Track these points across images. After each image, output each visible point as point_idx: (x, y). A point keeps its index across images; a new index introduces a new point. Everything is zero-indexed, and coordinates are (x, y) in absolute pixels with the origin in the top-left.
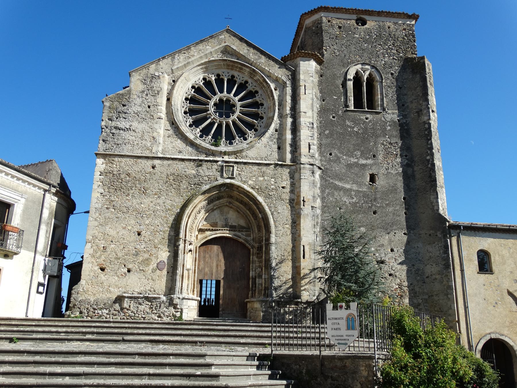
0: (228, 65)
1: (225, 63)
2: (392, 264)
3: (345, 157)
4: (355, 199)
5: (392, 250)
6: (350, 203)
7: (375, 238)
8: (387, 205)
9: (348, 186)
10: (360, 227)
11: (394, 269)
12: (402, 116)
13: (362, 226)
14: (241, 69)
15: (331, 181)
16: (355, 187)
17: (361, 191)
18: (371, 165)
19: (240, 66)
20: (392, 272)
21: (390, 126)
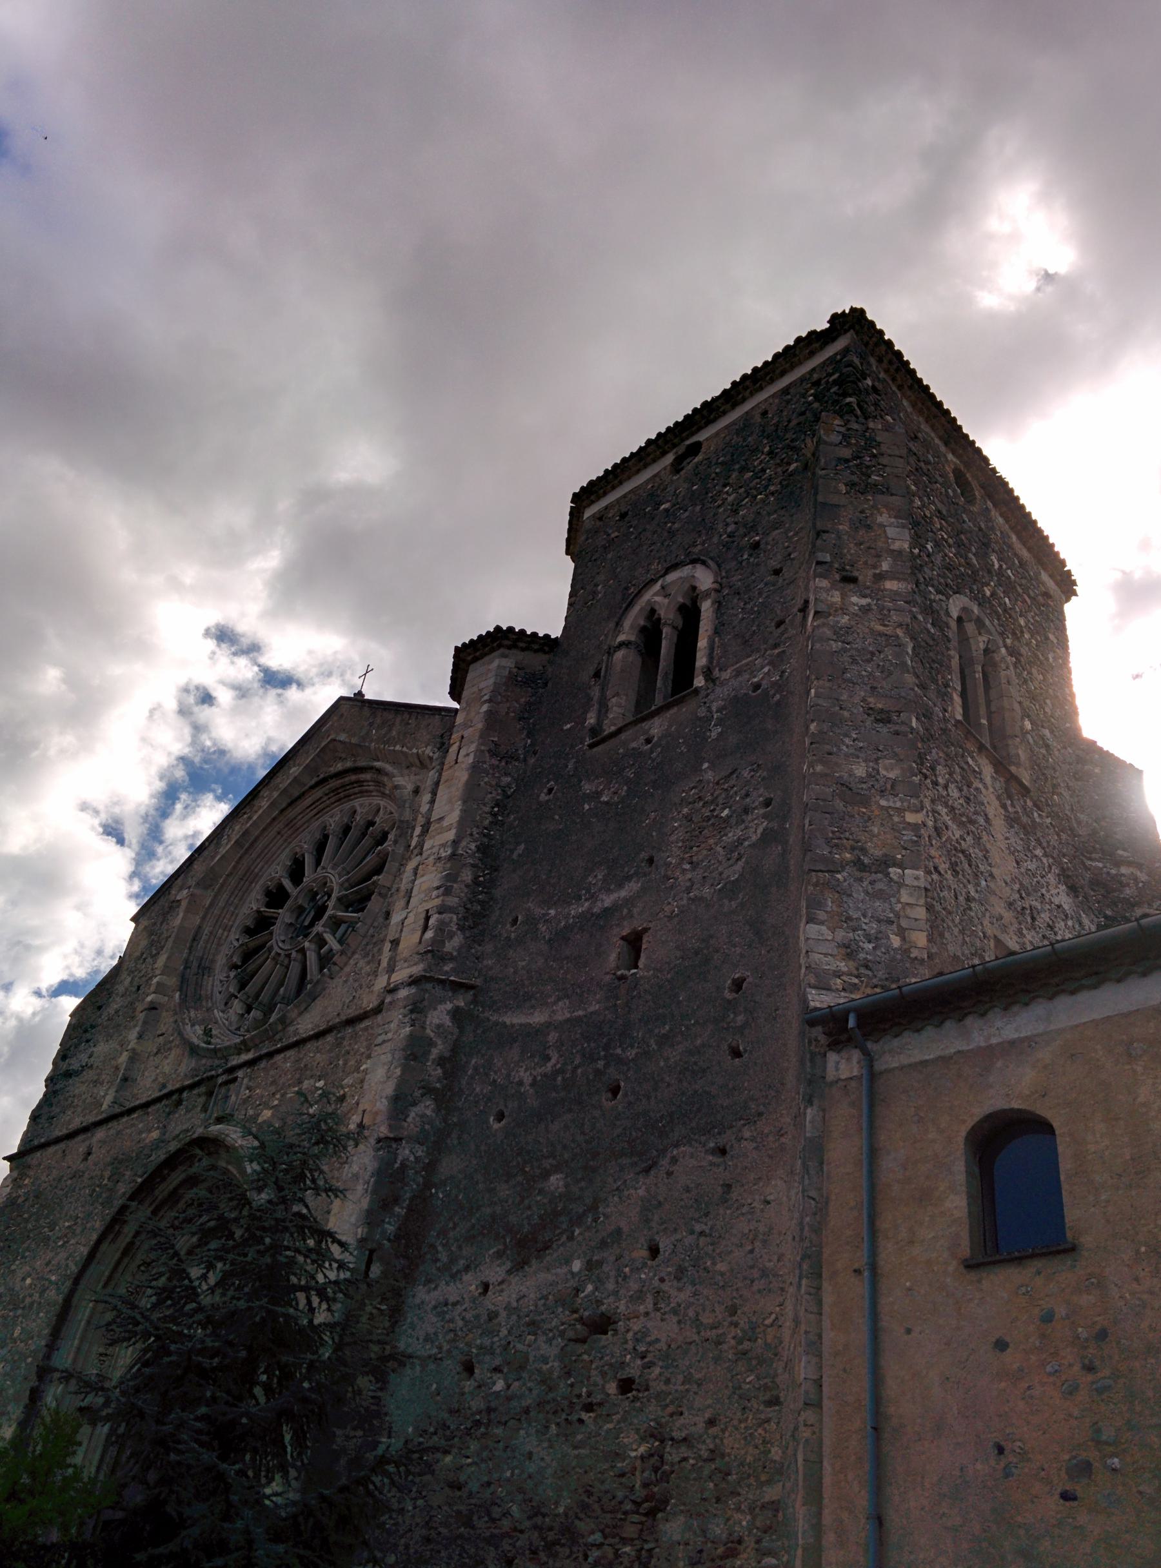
0: (335, 791)
1: (326, 788)
2: (636, 1326)
3: (552, 912)
4: (555, 1057)
5: (654, 1251)
6: (534, 1083)
7: (593, 1208)
8: (664, 1040)
9: (538, 1018)
10: (546, 1175)
11: (642, 1348)
12: (769, 664)
13: (557, 1169)
14: (360, 783)
15: (494, 1018)
16: (562, 1012)
17: (579, 1019)
18: (629, 902)
19: (353, 778)
20: (634, 1369)
21: (720, 722)
